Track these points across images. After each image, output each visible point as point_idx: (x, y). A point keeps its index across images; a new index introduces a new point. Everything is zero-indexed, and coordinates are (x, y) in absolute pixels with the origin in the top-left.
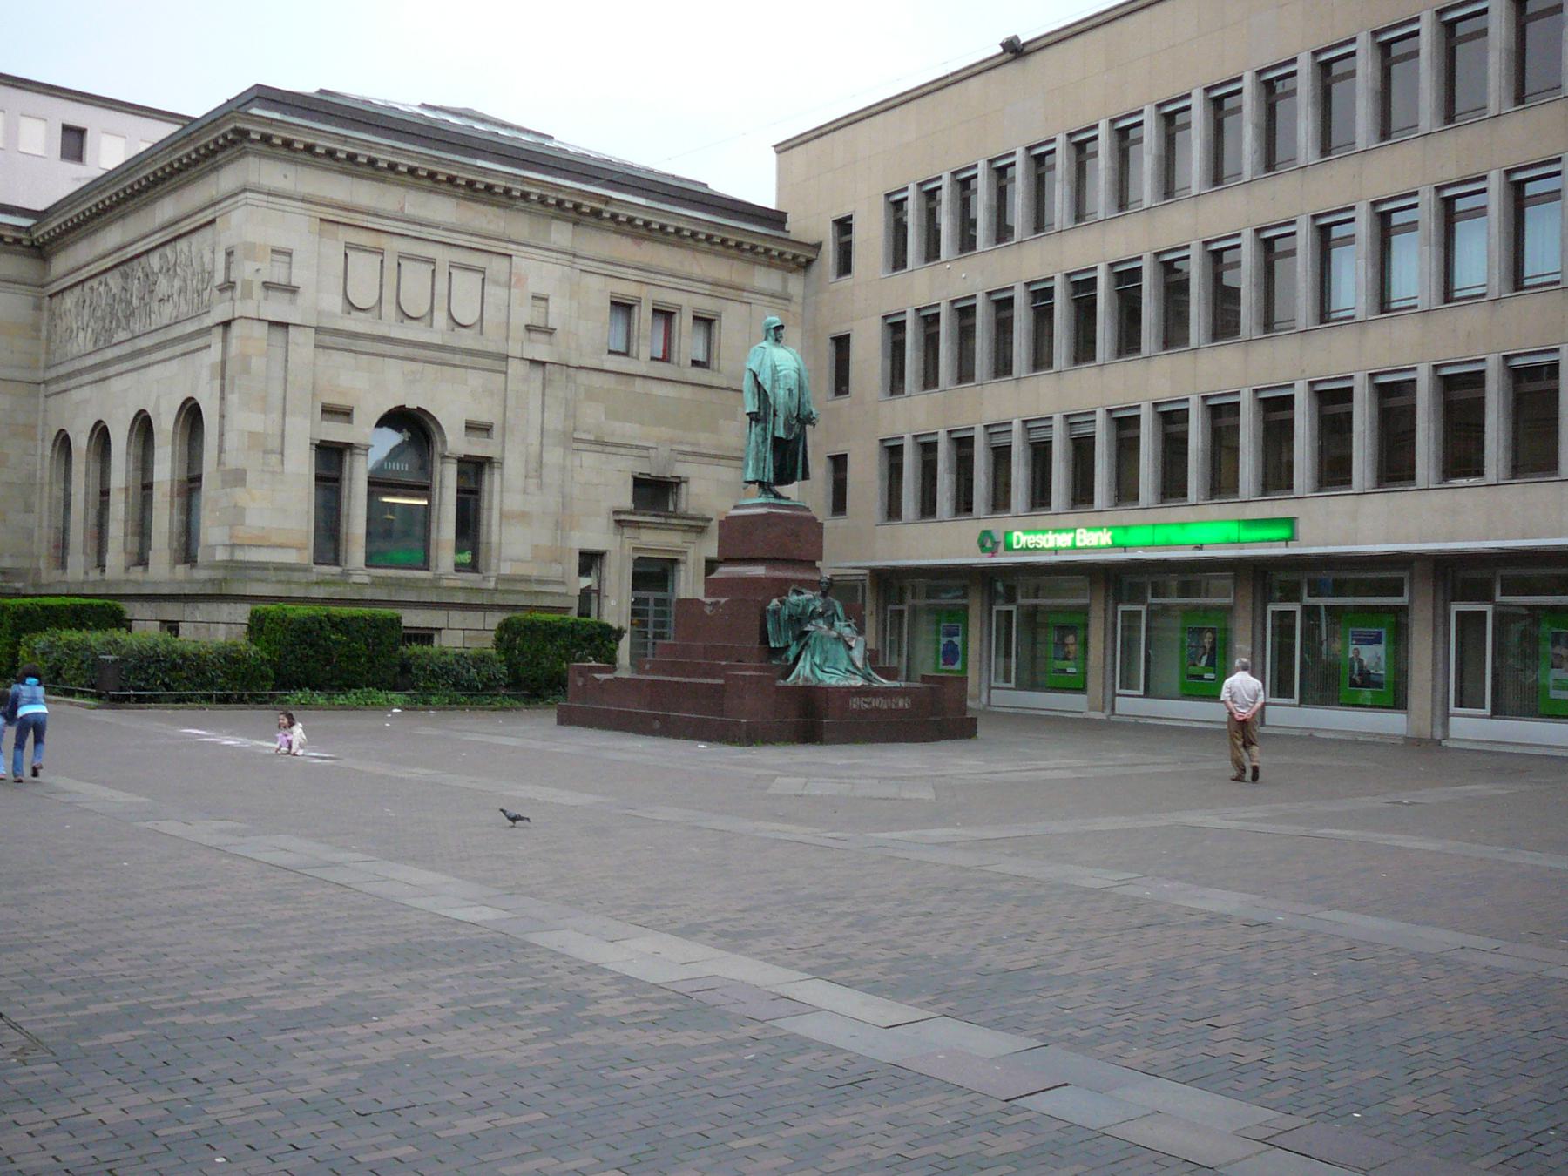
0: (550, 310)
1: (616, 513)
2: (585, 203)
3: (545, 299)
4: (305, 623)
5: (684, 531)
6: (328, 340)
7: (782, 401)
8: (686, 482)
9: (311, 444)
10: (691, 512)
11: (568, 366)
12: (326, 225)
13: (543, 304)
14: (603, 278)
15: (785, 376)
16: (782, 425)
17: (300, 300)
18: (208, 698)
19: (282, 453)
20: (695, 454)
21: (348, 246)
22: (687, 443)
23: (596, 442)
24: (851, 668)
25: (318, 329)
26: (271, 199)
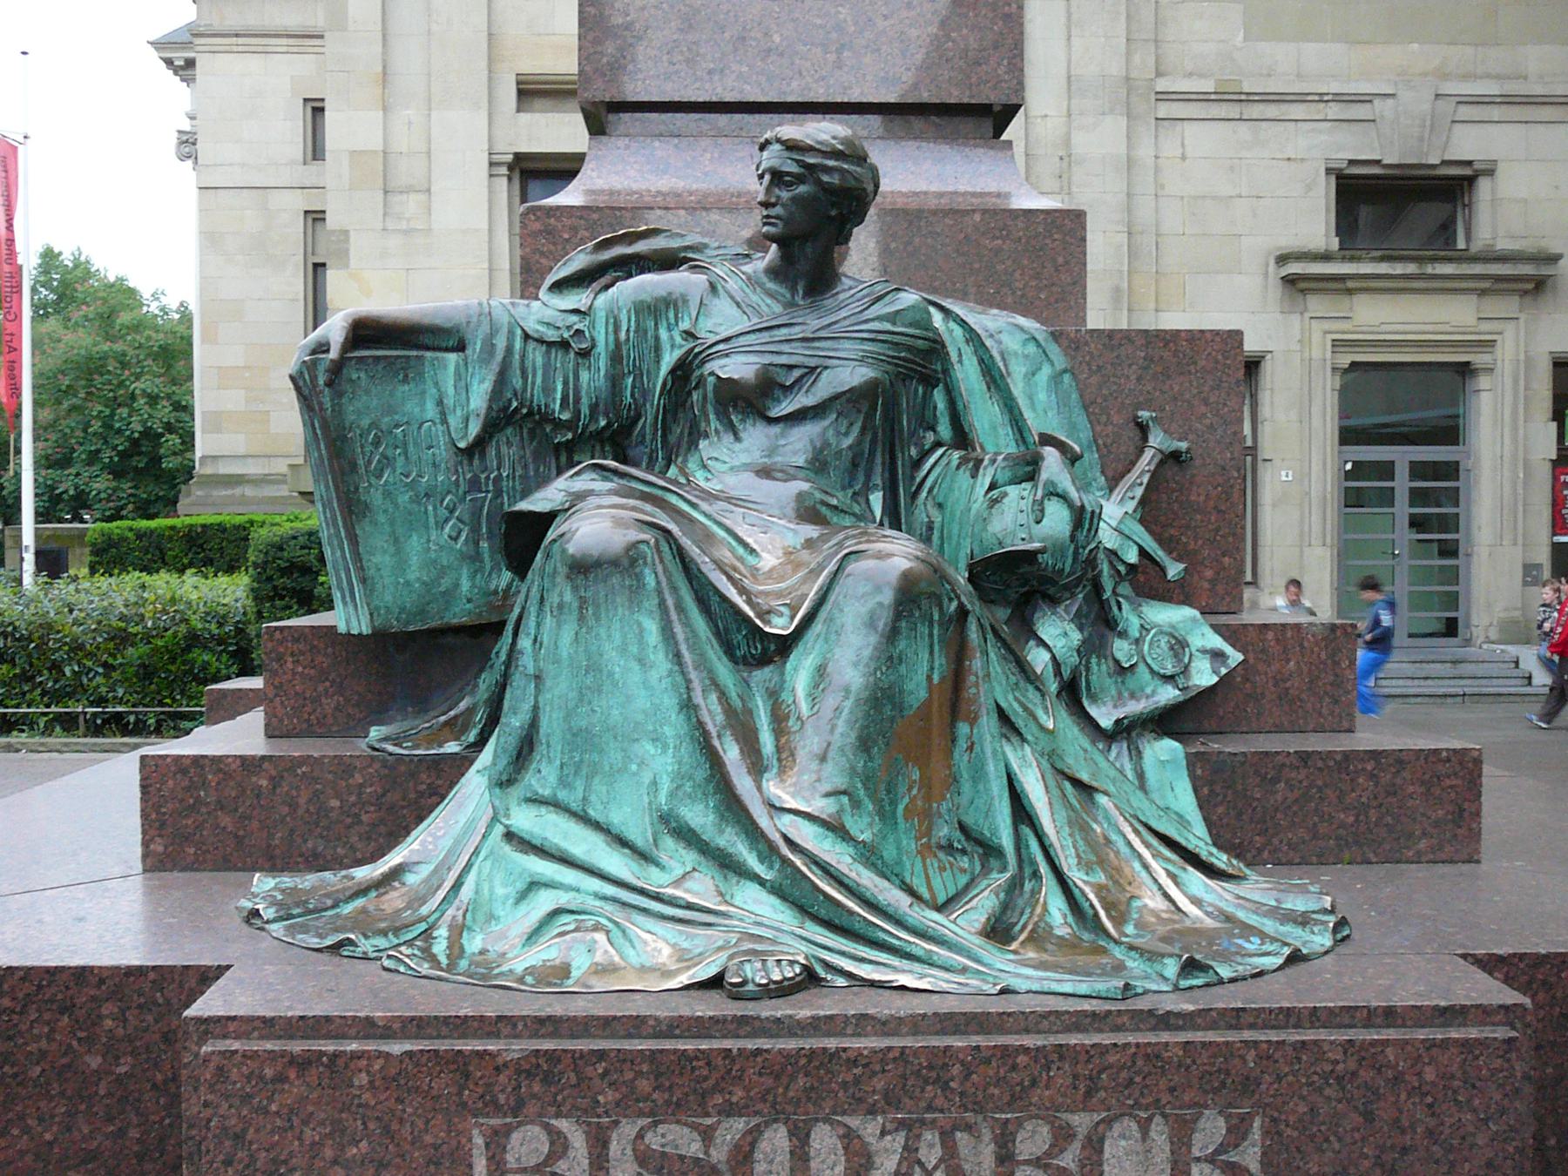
1: (1282, 259)
4: (281, 549)
5: (1483, 293)
8: (1490, 173)
9: (491, 164)
10: (1503, 245)
18: (68, 723)
19: (429, 190)
20: (1508, 100)
22: (1488, 76)
23: (1219, 97)
24: (699, 816)
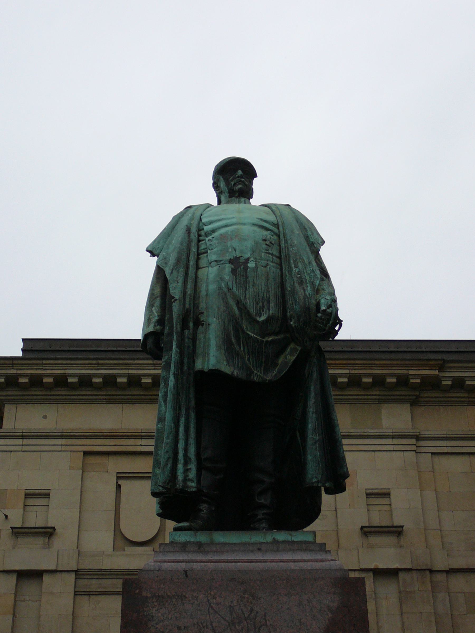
0: (393, 506)
2: (411, 372)
3: (386, 495)
6: (94, 584)
7: (212, 287)
11: (431, 571)
12: (92, 460)
13: (385, 501)
14: (466, 458)
15: (223, 238)
16: (213, 343)
17: (57, 543)
21: (121, 476)
25: (79, 574)
26: (26, 441)
